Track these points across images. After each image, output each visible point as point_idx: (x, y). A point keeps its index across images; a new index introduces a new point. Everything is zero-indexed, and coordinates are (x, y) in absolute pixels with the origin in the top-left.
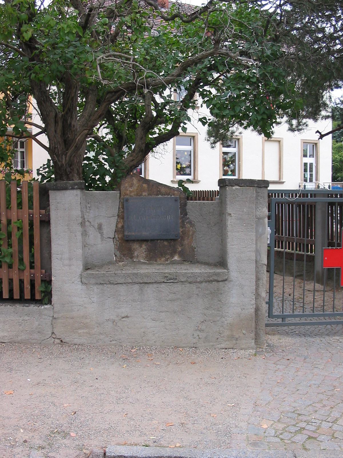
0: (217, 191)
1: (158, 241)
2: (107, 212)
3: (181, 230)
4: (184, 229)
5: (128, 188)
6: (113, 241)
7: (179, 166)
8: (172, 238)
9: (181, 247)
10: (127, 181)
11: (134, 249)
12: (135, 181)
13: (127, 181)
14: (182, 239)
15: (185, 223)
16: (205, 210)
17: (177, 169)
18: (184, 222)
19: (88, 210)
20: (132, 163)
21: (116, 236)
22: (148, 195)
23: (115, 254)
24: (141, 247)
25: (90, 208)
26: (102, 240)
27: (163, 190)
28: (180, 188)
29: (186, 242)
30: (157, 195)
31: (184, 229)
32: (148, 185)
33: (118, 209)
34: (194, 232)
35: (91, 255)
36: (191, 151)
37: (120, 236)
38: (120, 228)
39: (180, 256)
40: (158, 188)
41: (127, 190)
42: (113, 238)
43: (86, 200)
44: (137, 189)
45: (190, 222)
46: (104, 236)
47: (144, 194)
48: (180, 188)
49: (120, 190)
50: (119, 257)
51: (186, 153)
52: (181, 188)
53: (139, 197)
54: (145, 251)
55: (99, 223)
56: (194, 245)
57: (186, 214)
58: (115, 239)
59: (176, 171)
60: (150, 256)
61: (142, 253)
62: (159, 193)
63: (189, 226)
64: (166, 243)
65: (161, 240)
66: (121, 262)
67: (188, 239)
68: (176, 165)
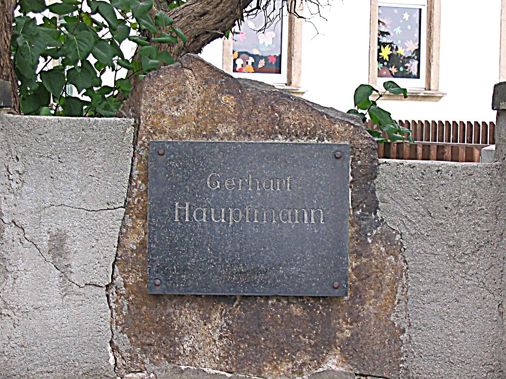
0: (491, 123)
1: (270, 302)
2: (84, 194)
3: (354, 264)
4: (365, 260)
5: (164, 106)
6: (108, 296)
7: (386, 52)
8: (317, 293)
9: (351, 324)
10: (162, 81)
11: (181, 327)
12: (192, 83)
13: (162, 81)
14: (358, 294)
15: (370, 241)
16: (442, 193)
17: (380, 60)
18: (366, 236)
19: (14, 185)
20: (199, 25)
21: (119, 279)
22: (239, 134)
23: (111, 342)
24: (207, 320)
25: (23, 178)
26: (66, 293)
27: (291, 117)
28: (360, 111)
29: (370, 307)
30: (271, 134)
31: (365, 260)
32: (240, 97)
33: (127, 182)
34: (400, 273)
35: (23, 346)
36: (420, 10)
37: (131, 281)
38: (133, 250)
39: (346, 358)
40: (273, 109)
41: (163, 115)
42: (107, 286)
43: (9, 146)
44: (198, 114)
45: (387, 238)
46: (73, 277)
47: (222, 130)
48: (360, 111)
49: (137, 117)
50: (125, 354)
51: (406, 16)
52: (364, 112)
53: (205, 140)
54: (221, 337)
55: (54, 233)
56: (397, 319)
57: (374, 207)
58: (114, 290)
59: (376, 65)
60: (237, 353)
61: (209, 344)
62: (277, 127)
63: (383, 249)
64: (296, 310)
65: (279, 298)
66: (135, 372)
67: (375, 297)
68: (377, 47)
